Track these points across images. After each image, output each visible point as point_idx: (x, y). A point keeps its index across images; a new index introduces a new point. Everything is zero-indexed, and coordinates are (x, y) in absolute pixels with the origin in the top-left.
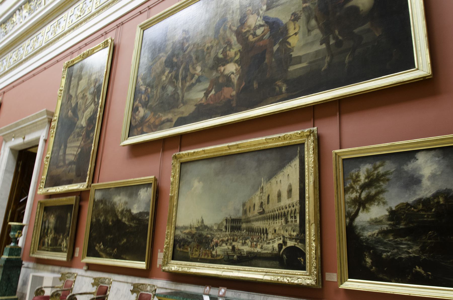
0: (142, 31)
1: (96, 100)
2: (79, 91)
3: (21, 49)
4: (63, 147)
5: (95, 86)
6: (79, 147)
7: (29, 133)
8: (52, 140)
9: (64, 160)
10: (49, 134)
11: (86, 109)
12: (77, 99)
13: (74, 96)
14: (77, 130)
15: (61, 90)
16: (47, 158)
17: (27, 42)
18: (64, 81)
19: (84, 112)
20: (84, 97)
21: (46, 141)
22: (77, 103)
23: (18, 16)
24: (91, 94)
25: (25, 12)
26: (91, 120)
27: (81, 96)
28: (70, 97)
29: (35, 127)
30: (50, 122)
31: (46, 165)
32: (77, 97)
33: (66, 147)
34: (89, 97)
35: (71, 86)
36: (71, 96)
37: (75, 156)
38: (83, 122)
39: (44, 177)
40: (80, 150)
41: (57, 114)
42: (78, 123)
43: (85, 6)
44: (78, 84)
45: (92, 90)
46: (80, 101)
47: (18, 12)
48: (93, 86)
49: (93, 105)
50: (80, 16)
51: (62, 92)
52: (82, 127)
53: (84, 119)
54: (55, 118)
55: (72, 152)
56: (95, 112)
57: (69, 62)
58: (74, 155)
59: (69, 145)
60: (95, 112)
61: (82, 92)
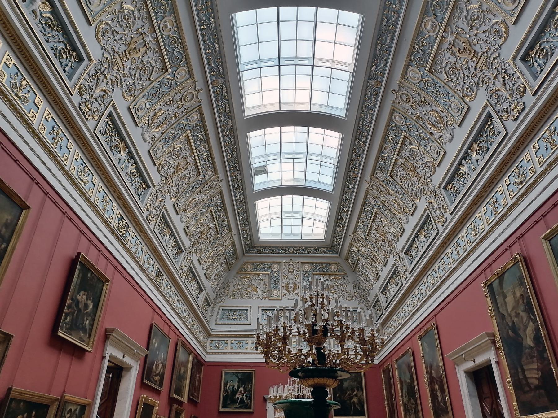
0: (548, 242)
1: (532, 317)
2: (509, 310)
3: (433, 272)
4: (520, 370)
5: (523, 302)
6: (538, 369)
7: (478, 354)
8: (504, 362)
9: (528, 385)
10: (497, 355)
11: (526, 327)
12: (511, 318)
13: (506, 314)
14: (527, 351)
15: (491, 310)
16: (509, 382)
17: (436, 265)
18: (489, 300)
19: (525, 331)
20: (517, 315)
21: (498, 363)
22: (513, 322)
23: (418, 243)
24: (523, 311)
25: (422, 238)
26: (537, 338)
27: (513, 314)
28: (503, 317)
29: (481, 350)
30: (494, 342)
31: (511, 390)
32: (510, 315)
33: (523, 370)
34: (523, 314)
35: (499, 305)
36: (503, 315)
37: (538, 379)
38: (529, 342)
39: (515, 404)
40: (540, 372)
41: (498, 335)
42: (524, 342)
43: (476, 224)
44: (505, 302)
45: (522, 307)
46: (515, 319)
47: (416, 239)
48: (521, 302)
49: (531, 323)
50: (476, 235)
51: (492, 311)
52: (531, 348)
53: (528, 339)
54: (498, 339)
55: (534, 375)
56: (537, 330)
57: (486, 282)
58: (536, 378)
59: (525, 367)
60: (537, 330)
61: (512, 310)
